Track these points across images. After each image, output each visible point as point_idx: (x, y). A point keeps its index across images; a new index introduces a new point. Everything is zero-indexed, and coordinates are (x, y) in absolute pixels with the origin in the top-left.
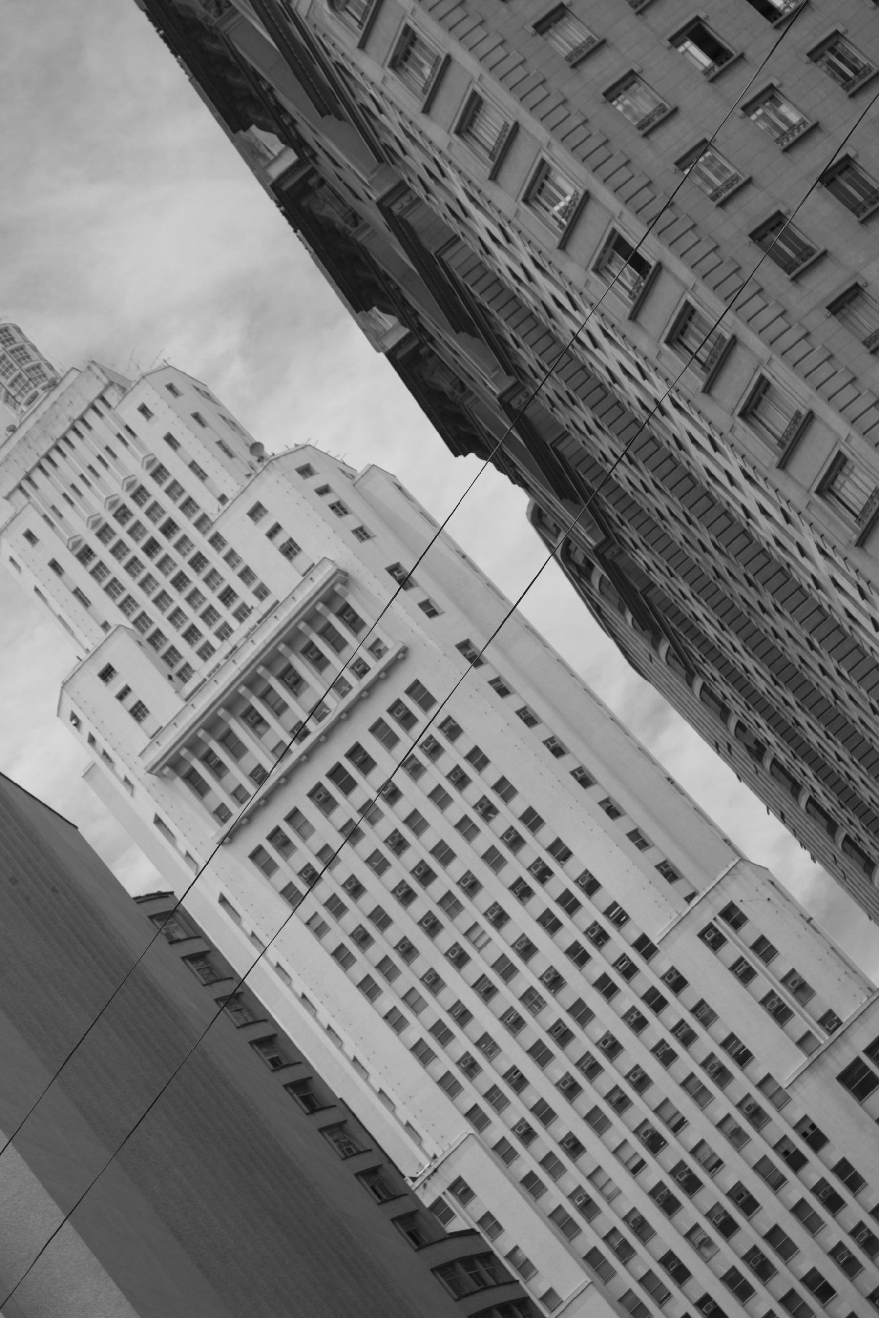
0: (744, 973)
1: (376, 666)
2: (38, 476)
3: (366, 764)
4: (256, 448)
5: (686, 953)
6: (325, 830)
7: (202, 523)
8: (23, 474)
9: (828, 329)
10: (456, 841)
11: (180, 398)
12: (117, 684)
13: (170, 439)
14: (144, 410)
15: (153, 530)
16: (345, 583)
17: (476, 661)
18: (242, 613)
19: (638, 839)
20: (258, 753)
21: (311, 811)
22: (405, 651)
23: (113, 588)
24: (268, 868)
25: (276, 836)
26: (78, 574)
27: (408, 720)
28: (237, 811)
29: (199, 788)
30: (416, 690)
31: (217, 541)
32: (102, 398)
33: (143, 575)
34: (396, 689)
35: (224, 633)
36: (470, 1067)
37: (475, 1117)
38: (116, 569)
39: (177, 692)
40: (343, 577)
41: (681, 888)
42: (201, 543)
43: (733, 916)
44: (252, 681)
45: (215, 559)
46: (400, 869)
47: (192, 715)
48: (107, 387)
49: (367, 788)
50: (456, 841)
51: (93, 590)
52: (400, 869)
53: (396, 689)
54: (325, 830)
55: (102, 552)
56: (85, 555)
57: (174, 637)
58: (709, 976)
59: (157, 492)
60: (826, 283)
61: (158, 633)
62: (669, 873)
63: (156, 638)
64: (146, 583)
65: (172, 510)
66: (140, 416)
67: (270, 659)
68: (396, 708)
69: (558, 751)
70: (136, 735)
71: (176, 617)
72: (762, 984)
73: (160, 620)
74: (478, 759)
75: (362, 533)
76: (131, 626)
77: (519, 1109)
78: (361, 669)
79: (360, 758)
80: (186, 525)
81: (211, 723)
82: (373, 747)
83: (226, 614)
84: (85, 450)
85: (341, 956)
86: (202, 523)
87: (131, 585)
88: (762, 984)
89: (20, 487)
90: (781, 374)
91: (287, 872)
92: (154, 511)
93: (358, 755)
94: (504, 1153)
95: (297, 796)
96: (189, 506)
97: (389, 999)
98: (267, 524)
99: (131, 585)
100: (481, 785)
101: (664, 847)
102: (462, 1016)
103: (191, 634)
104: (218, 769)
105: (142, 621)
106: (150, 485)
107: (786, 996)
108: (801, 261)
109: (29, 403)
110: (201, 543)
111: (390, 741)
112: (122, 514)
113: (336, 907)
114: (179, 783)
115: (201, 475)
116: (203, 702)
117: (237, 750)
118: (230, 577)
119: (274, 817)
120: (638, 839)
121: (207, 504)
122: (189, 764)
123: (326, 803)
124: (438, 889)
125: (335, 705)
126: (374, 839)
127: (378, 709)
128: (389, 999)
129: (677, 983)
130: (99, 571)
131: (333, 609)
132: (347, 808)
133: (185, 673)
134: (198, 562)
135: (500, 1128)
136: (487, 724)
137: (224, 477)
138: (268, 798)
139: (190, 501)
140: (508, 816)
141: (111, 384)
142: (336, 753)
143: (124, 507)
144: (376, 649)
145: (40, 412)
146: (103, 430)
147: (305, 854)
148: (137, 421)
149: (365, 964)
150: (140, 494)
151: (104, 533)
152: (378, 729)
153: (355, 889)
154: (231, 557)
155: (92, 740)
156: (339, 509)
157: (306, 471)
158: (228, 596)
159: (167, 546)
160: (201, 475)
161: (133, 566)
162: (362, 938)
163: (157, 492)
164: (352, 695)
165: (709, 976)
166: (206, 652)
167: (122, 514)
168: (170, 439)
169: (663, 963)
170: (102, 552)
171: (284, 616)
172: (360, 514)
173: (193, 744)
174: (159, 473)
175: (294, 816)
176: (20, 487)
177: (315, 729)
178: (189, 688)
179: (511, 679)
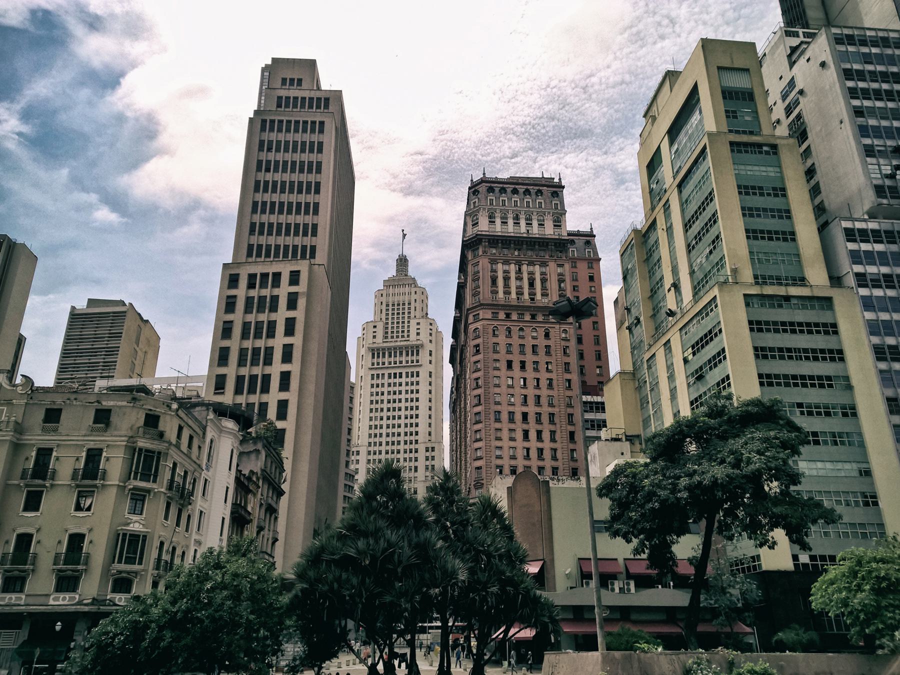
0: (427, 459)
1: (415, 364)
3: (401, 377)
4: (427, 314)
5: (421, 448)
6: (386, 381)
9: (492, 431)
10: (403, 401)
12: (375, 330)
15: (401, 312)
17: (430, 376)
18: (403, 337)
19: (430, 425)
21: (386, 376)
23: (387, 314)
24: (373, 379)
25: (378, 375)
26: (384, 307)
27: (412, 376)
28: (375, 366)
29: (373, 357)
30: (418, 373)
31: (409, 322)
34: (415, 370)
35: (397, 337)
36: (376, 436)
37: (370, 444)
38: (390, 312)
40: (422, 346)
41: (429, 438)
42: (406, 320)
43: (433, 449)
44: (395, 348)
45: (406, 325)
46: (391, 397)
47: (381, 345)
49: (397, 380)
50: (403, 401)
51: (384, 312)
52: (391, 397)
53: (415, 370)
54: (386, 381)
55: (390, 308)
56: (388, 305)
57: (390, 330)
58: (422, 455)
59: (406, 306)
60: (498, 425)
62: (430, 434)
64: (393, 318)
65: (406, 311)
67: (401, 347)
68: (412, 372)
69: (430, 401)
70: (371, 340)
71: (393, 328)
72: (428, 463)
73: (390, 326)
74: (417, 392)
75: (431, 341)
77: (377, 448)
78: (412, 362)
80: (406, 315)
81: (384, 349)
82: (404, 375)
83: (400, 334)
84: (402, 290)
85: (372, 402)
86: (409, 317)
87: (390, 317)
88: (428, 463)
90: (483, 431)
91: (375, 382)
92: (403, 309)
93: (401, 374)
94: (369, 453)
95: (386, 372)
96: (409, 313)
97: (372, 415)
99: (390, 317)
100: (414, 396)
101: (433, 430)
102: (381, 427)
103: (393, 332)
104: (378, 357)
105: (387, 323)
107: (430, 468)
108: (498, 420)
110: (406, 320)
111: (407, 377)
112: (398, 305)
113: (377, 394)
116: (385, 345)
117: (384, 356)
119: (380, 372)
120: (430, 425)
121: (412, 315)
122: (375, 352)
123: (390, 377)
124: (395, 397)
125: (404, 364)
126: (391, 389)
127: (410, 370)
128: (372, 415)
129: (416, 451)
130: (387, 310)
131: (416, 349)
132: (392, 381)
134: (403, 322)
135: (371, 449)
136: (423, 388)
137: (418, 313)
138: (382, 368)
140: (414, 404)
142: (398, 371)
144: (418, 361)
146: (407, 289)
147: (380, 382)
148: (413, 293)
149: (374, 406)
150: (404, 304)
151: (393, 305)
152: (407, 373)
153: (383, 394)
154: (409, 326)
156: (431, 334)
157: (431, 324)
158: (403, 332)
159: (401, 316)
161: (393, 314)
162: (377, 402)
163: (406, 306)
165: (422, 455)
166: (392, 337)
167: (398, 305)
169: (417, 446)
170: (390, 308)
171: (409, 343)
172: (433, 338)
173: (378, 350)
174: (409, 304)
175: (383, 374)
177: (398, 364)
179: (433, 384)
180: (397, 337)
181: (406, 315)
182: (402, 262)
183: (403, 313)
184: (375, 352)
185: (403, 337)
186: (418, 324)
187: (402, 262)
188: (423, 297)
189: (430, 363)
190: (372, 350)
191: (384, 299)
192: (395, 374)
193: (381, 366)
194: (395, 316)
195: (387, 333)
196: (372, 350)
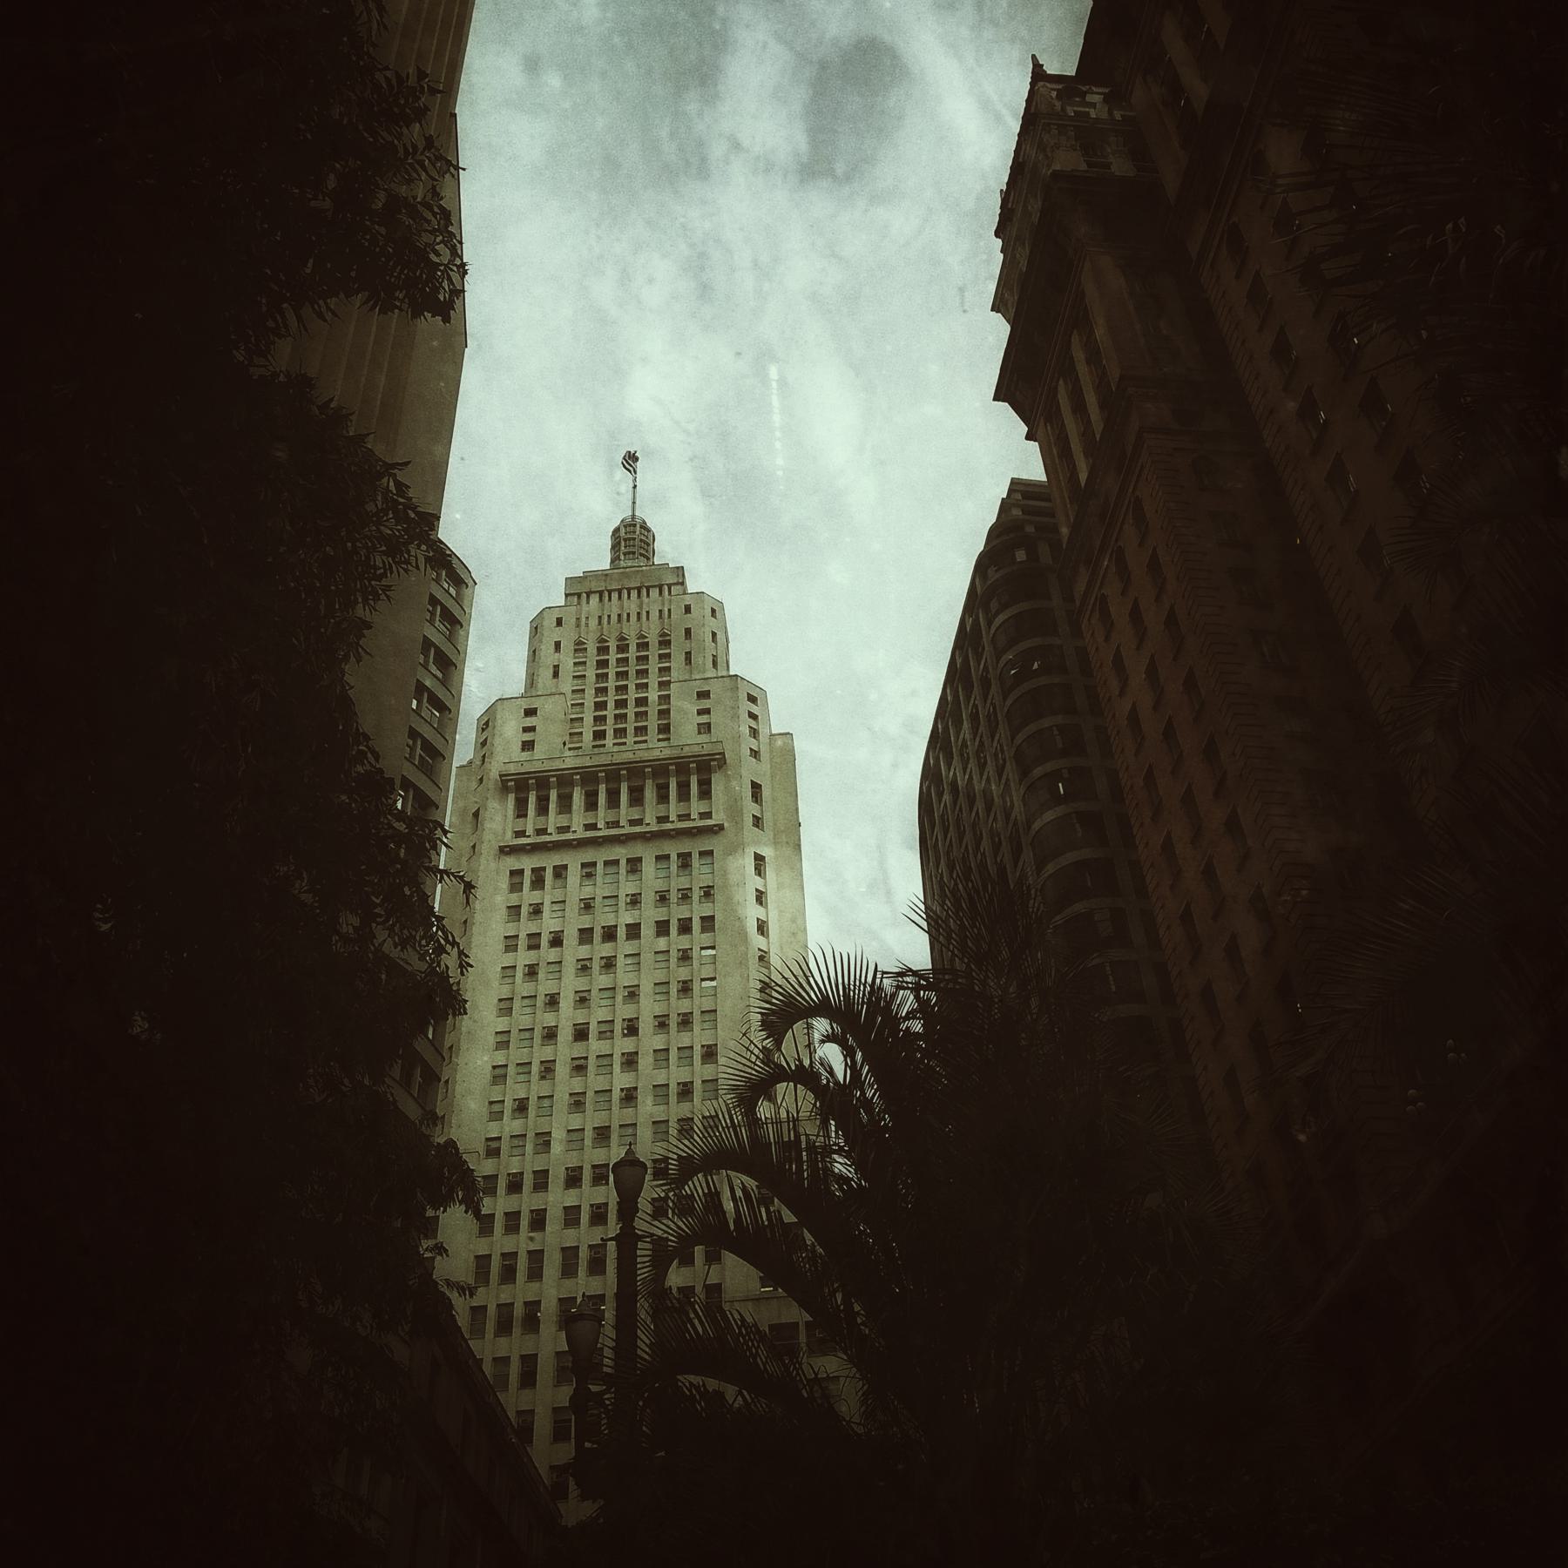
2: (595, 599)
12: (530, 721)
16: (720, 767)
20: (578, 820)
22: (721, 827)
24: (516, 887)
26: (567, 660)
29: (521, 813)
34: (694, 846)
59: (654, 652)
75: (755, 754)
80: (653, 680)
86: (664, 685)
89: (579, 595)
96: (665, 671)
112: (623, 648)
114: (511, 797)
119: (549, 861)
155: (484, 743)
157: (752, 699)
163: (654, 652)
170: (592, 655)
174: (665, 643)
176: (579, 595)
182: (632, 539)
187: (632, 539)
188: (712, 624)
189: (757, 822)
191: (567, 636)
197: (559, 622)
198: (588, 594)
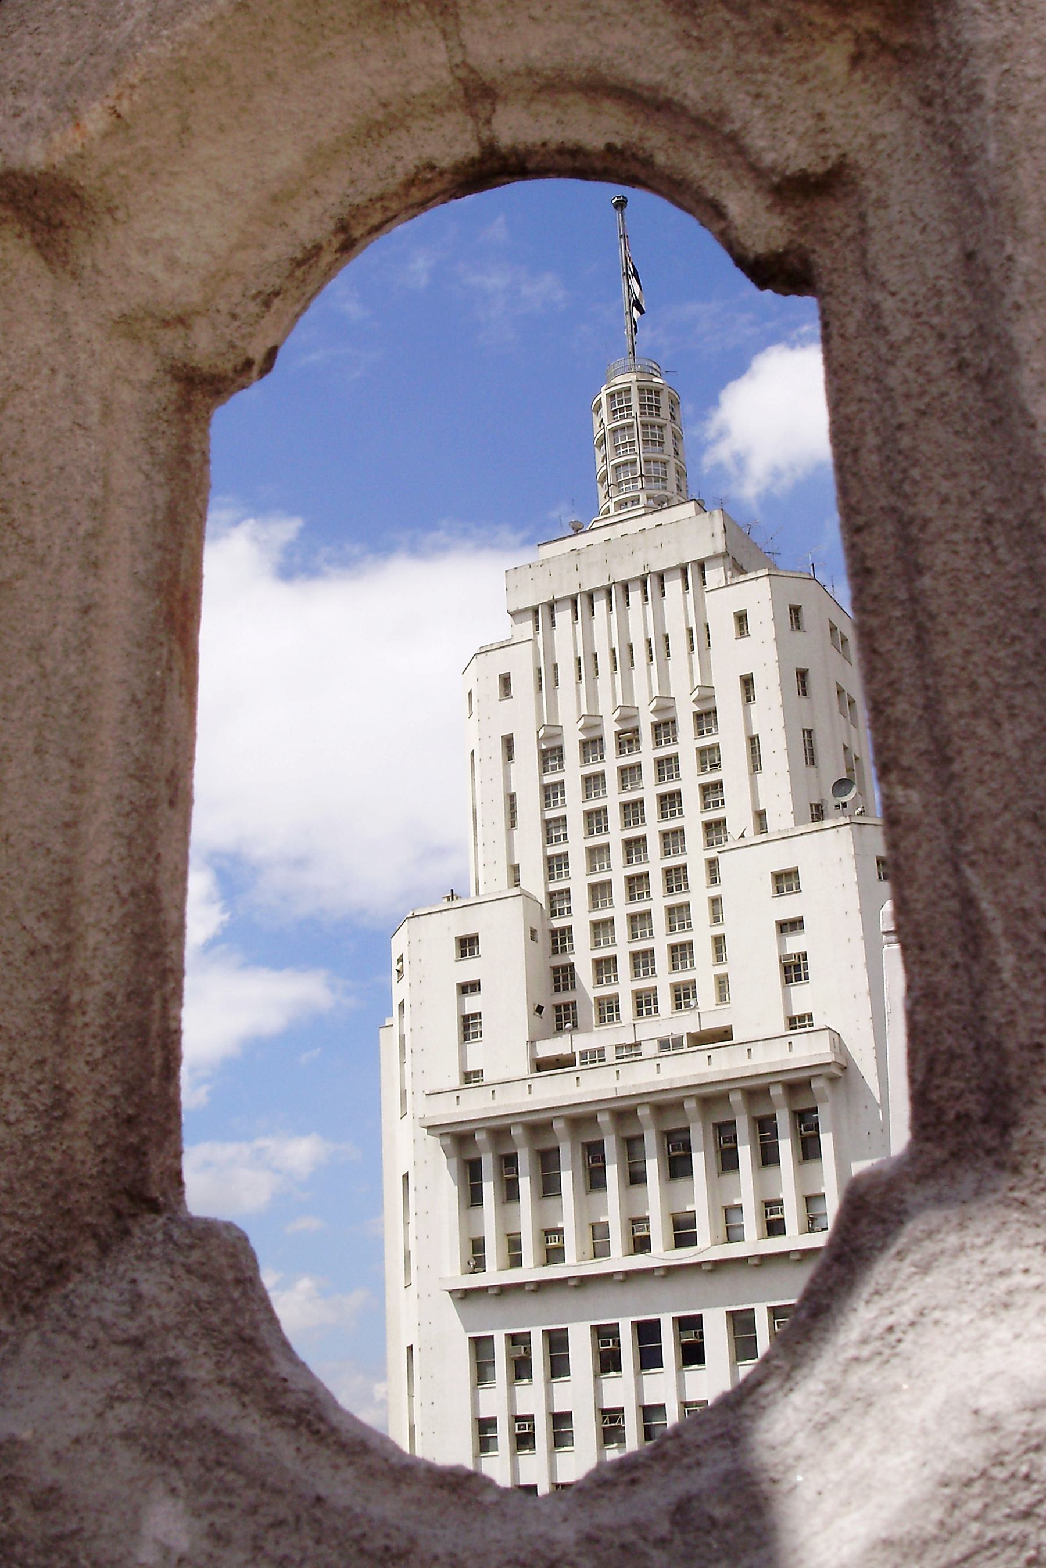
7: (714, 829)
8: (548, 598)
11: (798, 634)
12: (469, 970)
13: (747, 682)
14: (741, 619)
24: (482, 1372)
28: (494, 1274)
29: (474, 1197)
32: (701, 565)
33: (598, 840)
38: (574, 807)
39: (532, 1042)
44: (623, 1113)
48: (715, 557)
55: (572, 771)
56: (551, 755)
59: (686, 744)
61: (566, 932)
63: (560, 939)
65: (689, 781)
66: (731, 623)
73: (580, 918)
76: (542, 898)
79: (690, 1338)
80: (692, 817)
86: (714, 829)
87: (577, 843)
96: (712, 791)
98: (788, 907)
99: (577, 843)
105: (558, 901)
106: (686, 724)
109: (621, 504)
110: (695, 854)
112: (628, 740)
115: (756, 765)
118: (700, 934)
121: (736, 813)
123: (608, 1362)
133: (564, 1017)
139: (717, 786)
141: (725, 555)
143: (636, 730)
145: (620, 529)
148: (723, 627)
150: (664, 729)
151: (592, 746)
160: (756, 765)
161: (596, 820)
164: (735, 1251)
167: (628, 740)
168: (747, 682)
170: (572, 771)
173: (499, 1133)
174: (705, 719)
178: (548, 1049)
180: (645, 1003)
181: (692, 817)
183: (670, 802)
184: (486, 1156)
185: (683, 995)
186: (785, 881)
190: (460, 1140)
191: (521, 718)
192: (647, 1333)
193: (531, 1271)
194: (615, 835)
195: (563, 977)
196: (460, 1140)
197: (506, 681)
198: (552, 606)
